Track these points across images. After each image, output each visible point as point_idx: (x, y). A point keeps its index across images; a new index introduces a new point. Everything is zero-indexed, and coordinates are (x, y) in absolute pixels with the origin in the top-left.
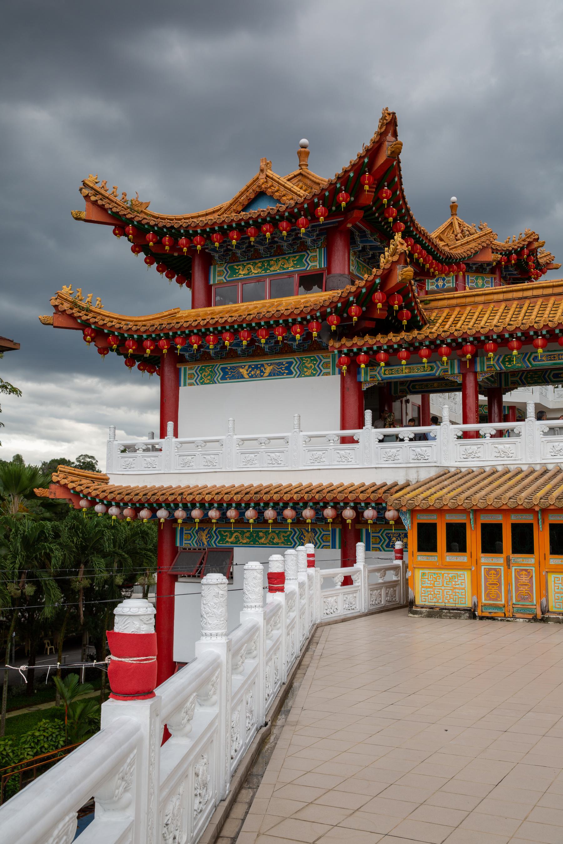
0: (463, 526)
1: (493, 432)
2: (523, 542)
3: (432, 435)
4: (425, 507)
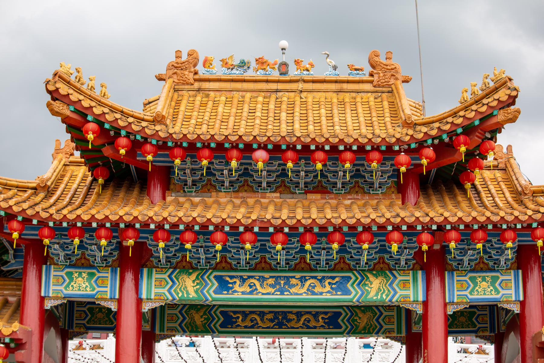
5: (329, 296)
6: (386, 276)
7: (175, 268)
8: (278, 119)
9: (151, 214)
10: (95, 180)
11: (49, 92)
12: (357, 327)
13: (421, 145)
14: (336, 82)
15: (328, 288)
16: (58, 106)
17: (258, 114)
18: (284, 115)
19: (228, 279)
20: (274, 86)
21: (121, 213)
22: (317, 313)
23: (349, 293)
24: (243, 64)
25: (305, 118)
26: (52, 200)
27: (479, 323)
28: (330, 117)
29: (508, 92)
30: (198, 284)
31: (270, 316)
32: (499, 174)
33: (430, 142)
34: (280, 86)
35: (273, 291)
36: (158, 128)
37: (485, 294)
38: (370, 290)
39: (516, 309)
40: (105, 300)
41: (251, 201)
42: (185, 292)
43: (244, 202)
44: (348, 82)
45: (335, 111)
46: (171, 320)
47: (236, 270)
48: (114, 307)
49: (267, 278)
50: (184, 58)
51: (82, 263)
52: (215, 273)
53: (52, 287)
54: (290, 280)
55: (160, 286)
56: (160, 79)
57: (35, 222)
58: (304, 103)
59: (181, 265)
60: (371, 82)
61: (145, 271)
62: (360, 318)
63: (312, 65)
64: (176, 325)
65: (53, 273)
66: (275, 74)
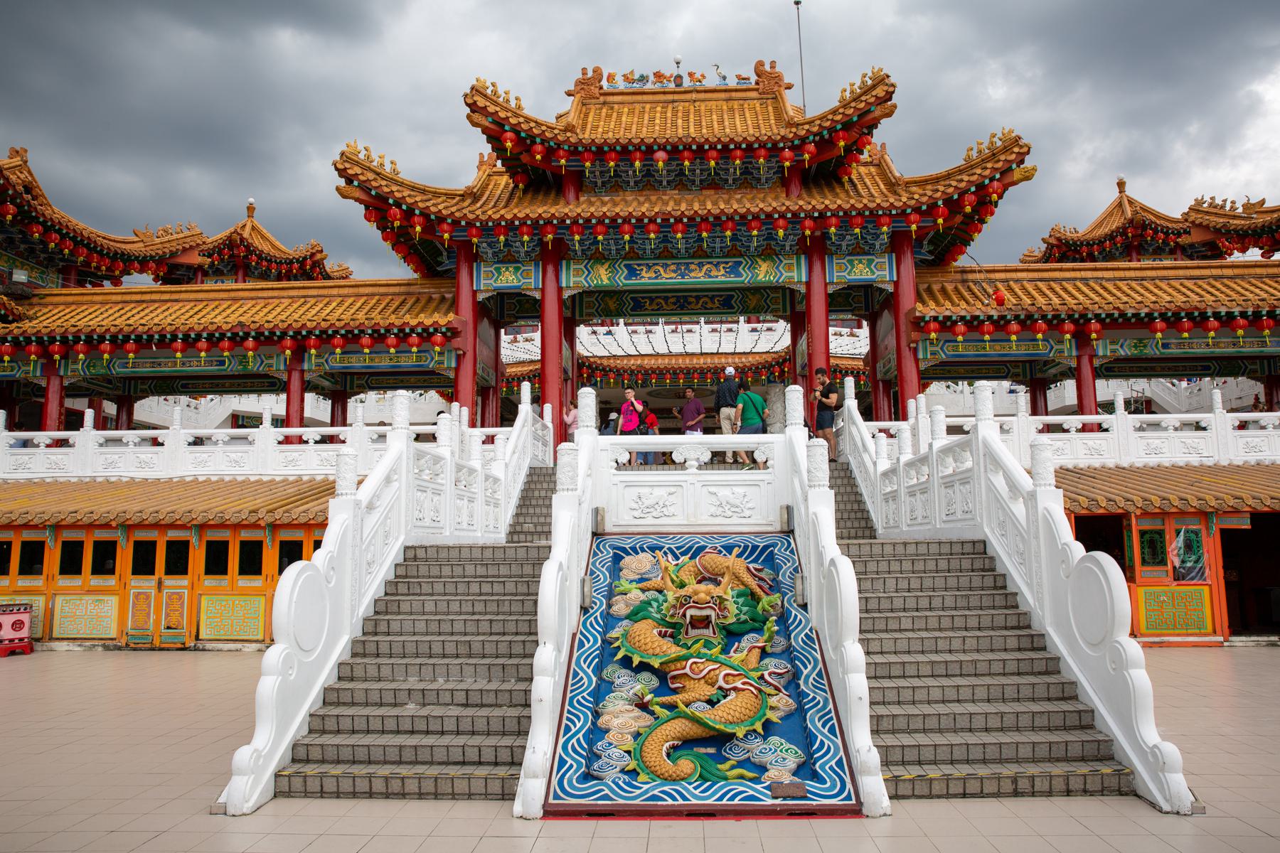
0: (259, 544)
1: (48, 441)
2: (178, 562)
3: (71, 441)
4: (236, 521)
5: (723, 279)
6: (773, 261)
8: (674, 125)
9: (566, 210)
10: (516, 186)
11: (468, 105)
13: (803, 140)
14: (725, 91)
15: (722, 272)
16: (476, 117)
17: (657, 121)
18: (680, 121)
20: (670, 97)
21: (540, 211)
23: (741, 275)
24: (643, 79)
25: (699, 124)
26: (478, 205)
28: (721, 122)
29: (886, 88)
32: (873, 169)
33: (811, 138)
34: (676, 97)
36: (569, 134)
39: (890, 288)
40: (530, 290)
41: (653, 198)
43: (648, 200)
44: (736, 90)
45: (726, 116)
46: (589, 307)
47: (642, 259)
48: (538, 296)
50: (590, 74)
51: (508, 258)
53: (483, 282)
55: (577, 275)
56: (569, 94)
57: (463, 223)
58: (698, 111)
59: (596, 257)
60: (757, 90)
61: (564, 263)
63: (703, 76)
65: (483, 269)
66: (672, 86)
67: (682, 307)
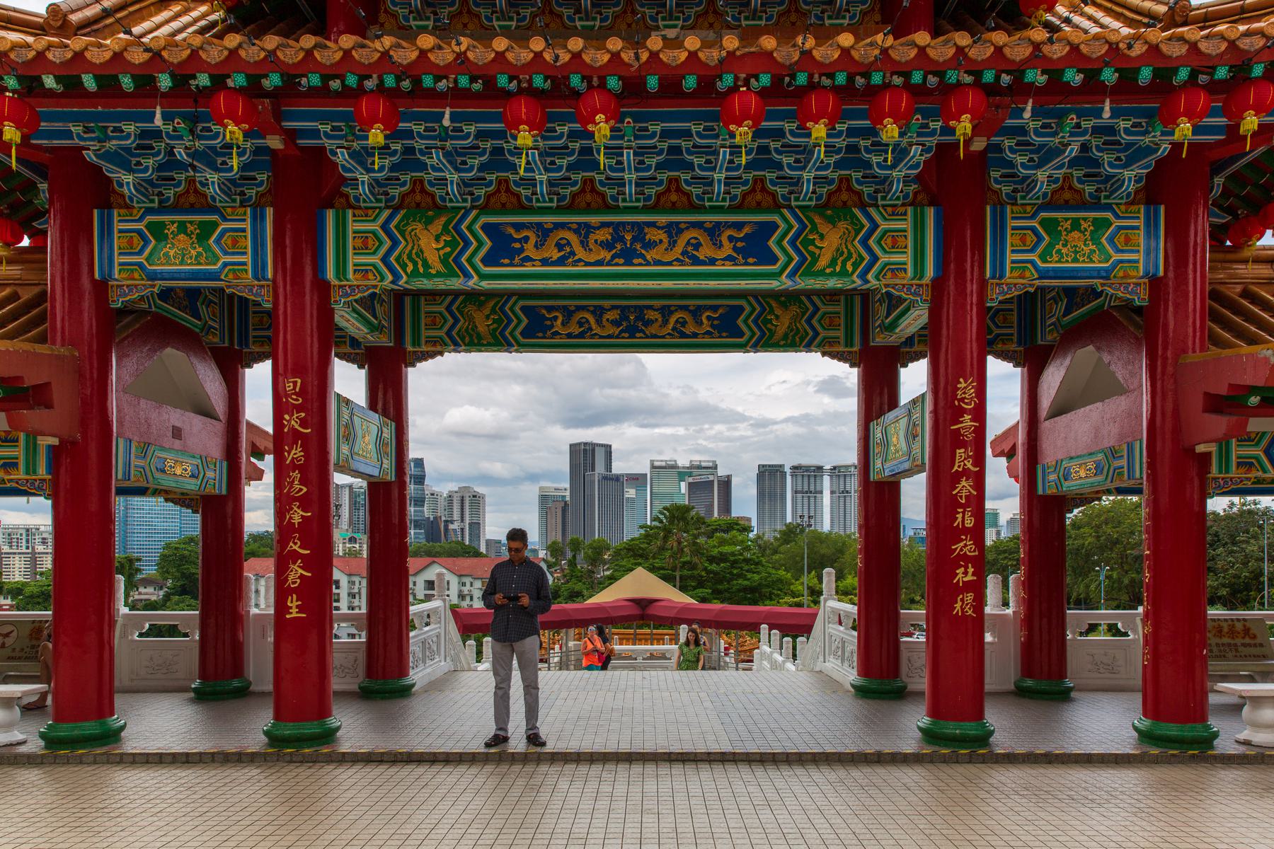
7: (396, 209)
12: (772, 333)
15: (727, 249)
19: (511, 231)
22: (699, 307)
27: (998, 327)
30: (447, 244)
31: (612, 315)
35: (609, 258)
37: (1076, 260)
38: (817, 252)
42: (420, 263)
46: (433, 324)
49: (595, 228)
52: (484, 219)
54: (646, 230)
62: (777, 317)
64: (442, 333)
67: (632, 331)
